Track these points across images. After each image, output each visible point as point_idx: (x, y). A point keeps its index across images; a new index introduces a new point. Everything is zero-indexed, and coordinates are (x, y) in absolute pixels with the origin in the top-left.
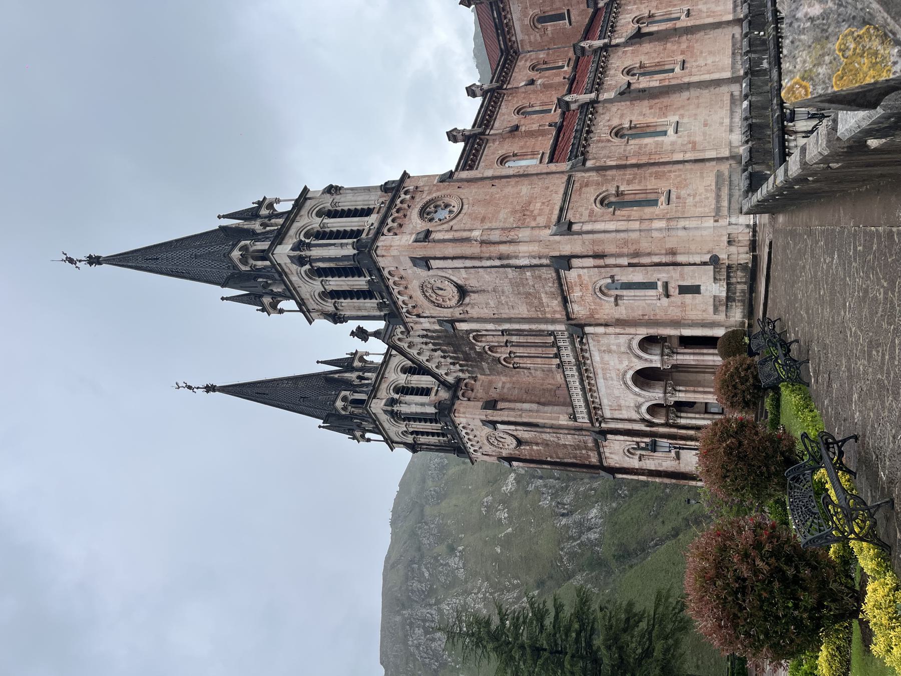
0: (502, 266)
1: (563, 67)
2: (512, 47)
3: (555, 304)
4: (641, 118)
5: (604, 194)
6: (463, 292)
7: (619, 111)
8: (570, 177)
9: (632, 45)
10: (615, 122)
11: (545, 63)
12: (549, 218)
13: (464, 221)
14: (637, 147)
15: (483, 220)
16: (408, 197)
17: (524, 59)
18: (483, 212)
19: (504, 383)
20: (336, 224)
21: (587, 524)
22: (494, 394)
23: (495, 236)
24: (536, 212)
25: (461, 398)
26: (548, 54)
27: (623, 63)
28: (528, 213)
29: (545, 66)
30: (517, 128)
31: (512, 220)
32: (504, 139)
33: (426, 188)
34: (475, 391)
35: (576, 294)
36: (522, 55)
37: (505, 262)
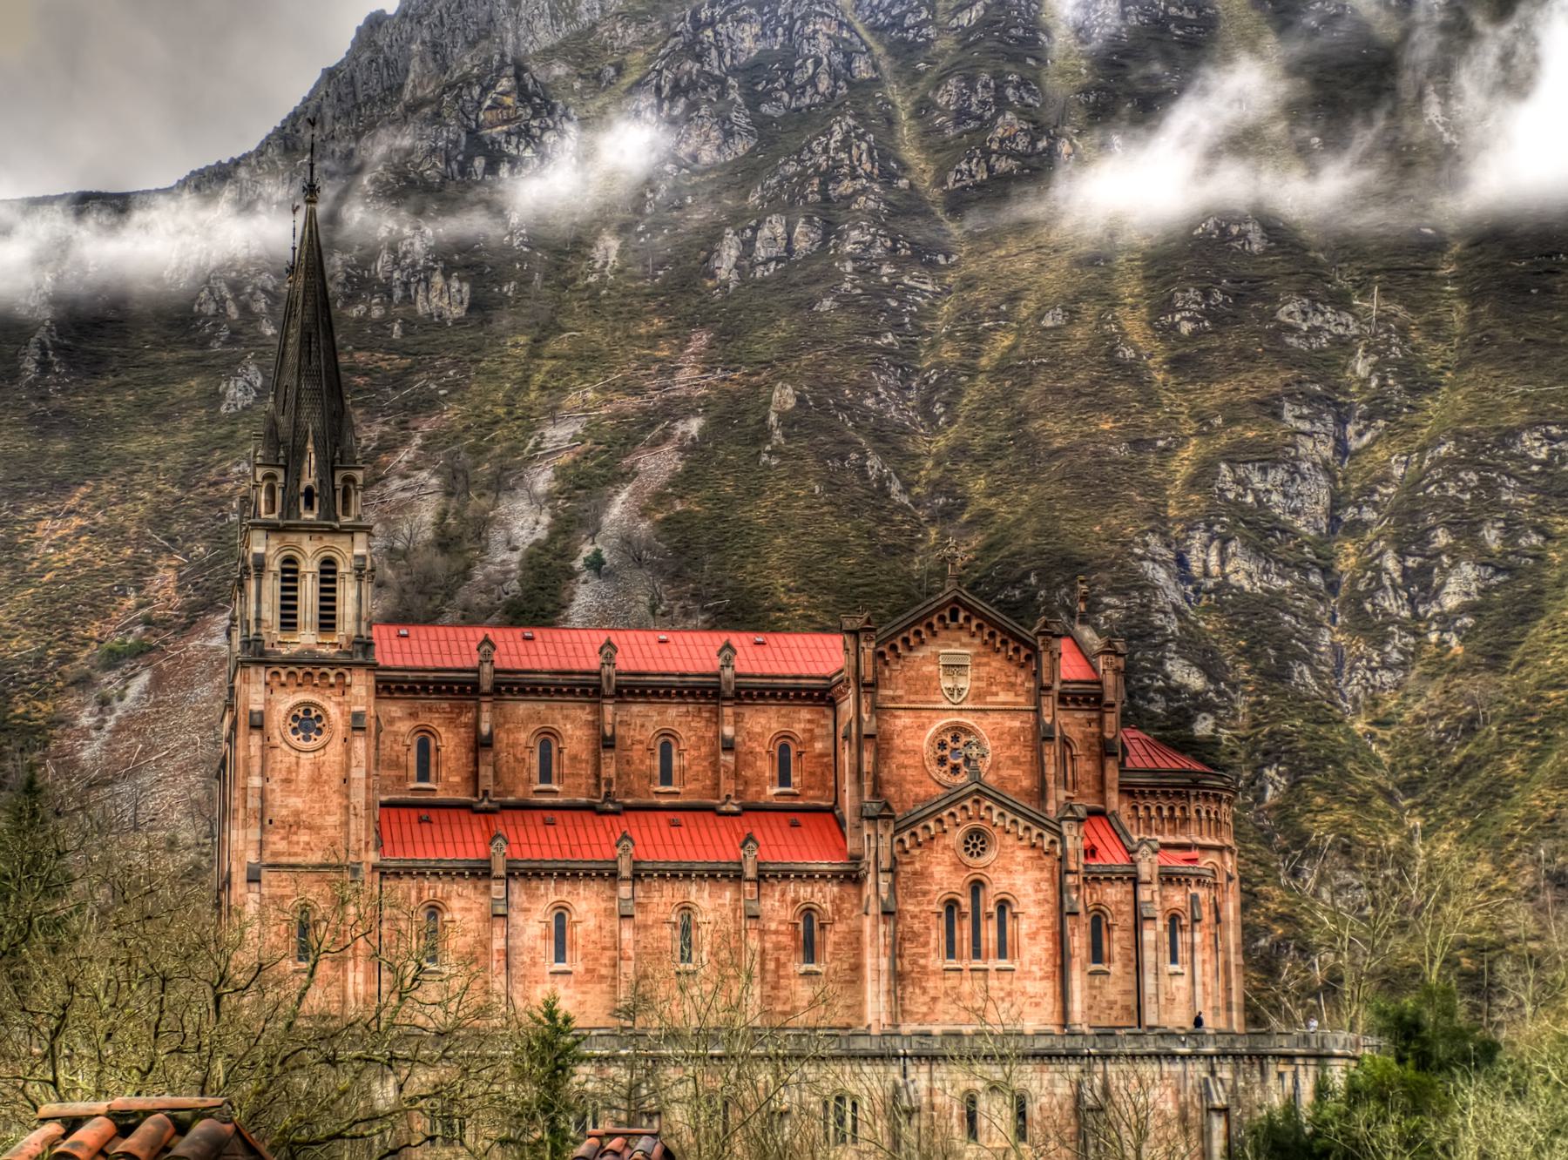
1: (784, 780)
11: (800, 754)
12: (283, 854)
16: (332, 680)
17: (815, 716)
20: (309, 591)
21: (1144, 658)
24: (295, 838)
28: (294, 829)
31: (284, 812)
33: (347, 698)
36: (829, 712)
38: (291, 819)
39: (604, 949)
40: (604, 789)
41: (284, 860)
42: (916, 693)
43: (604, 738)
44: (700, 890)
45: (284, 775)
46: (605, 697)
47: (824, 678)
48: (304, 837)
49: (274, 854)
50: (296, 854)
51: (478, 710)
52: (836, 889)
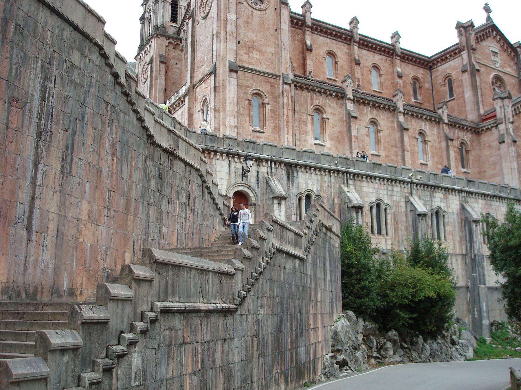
0: (213, 36)
2: (434, 64)
3: (199, 75)
4: (331, 125)
5: (263, 95)
6: (205, 18)
7: (338, 113)
8: (279, 77)
9: (398, 126)
10: (328, 109)
13: (246, 11)
14: (305, 120)
15: (247, 23)
17: (425, 73)
18: (254, 23)
19: (180, 69)
22: (172, 62)
23: (231, 28)
24: (251, 55)
25: (168, 41)
26: (428, 89)
27: (383, 120)
28: (251, 49)
29: (417, 87)
30: (358, 64)
31: (246, 40)
32: (351, 56)
34: (174, 50)
35: (204, 86)
36: (428, 72)
37: (215, 36)
38: (250, 44)
39: (392, 146)
40: (357, 83)
41: (246, 65)
42: (485, 59)
43: (355, 59)
44: (425, 125)
45: (245, 19)
46: (355, 42)
47: (428, 57)
48: (256, 55)
49: (240, 61)
50: (252, 64)
51: (304, 34)
52: (470, 136)
